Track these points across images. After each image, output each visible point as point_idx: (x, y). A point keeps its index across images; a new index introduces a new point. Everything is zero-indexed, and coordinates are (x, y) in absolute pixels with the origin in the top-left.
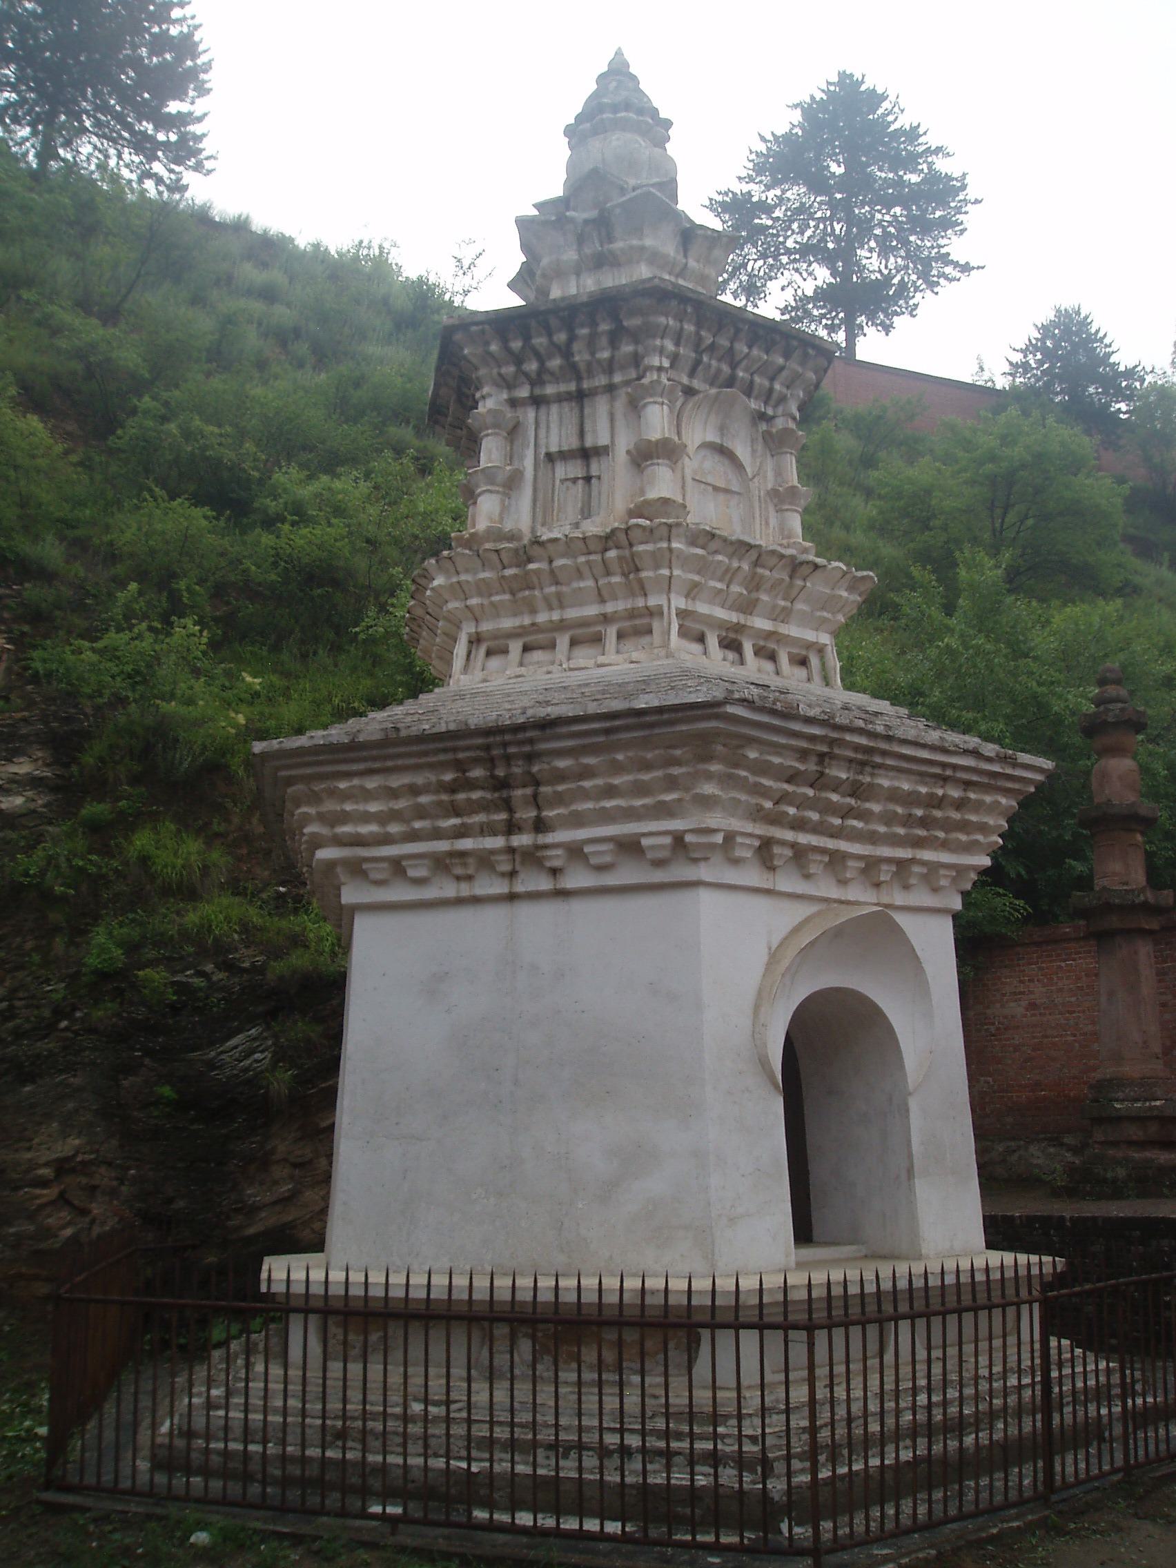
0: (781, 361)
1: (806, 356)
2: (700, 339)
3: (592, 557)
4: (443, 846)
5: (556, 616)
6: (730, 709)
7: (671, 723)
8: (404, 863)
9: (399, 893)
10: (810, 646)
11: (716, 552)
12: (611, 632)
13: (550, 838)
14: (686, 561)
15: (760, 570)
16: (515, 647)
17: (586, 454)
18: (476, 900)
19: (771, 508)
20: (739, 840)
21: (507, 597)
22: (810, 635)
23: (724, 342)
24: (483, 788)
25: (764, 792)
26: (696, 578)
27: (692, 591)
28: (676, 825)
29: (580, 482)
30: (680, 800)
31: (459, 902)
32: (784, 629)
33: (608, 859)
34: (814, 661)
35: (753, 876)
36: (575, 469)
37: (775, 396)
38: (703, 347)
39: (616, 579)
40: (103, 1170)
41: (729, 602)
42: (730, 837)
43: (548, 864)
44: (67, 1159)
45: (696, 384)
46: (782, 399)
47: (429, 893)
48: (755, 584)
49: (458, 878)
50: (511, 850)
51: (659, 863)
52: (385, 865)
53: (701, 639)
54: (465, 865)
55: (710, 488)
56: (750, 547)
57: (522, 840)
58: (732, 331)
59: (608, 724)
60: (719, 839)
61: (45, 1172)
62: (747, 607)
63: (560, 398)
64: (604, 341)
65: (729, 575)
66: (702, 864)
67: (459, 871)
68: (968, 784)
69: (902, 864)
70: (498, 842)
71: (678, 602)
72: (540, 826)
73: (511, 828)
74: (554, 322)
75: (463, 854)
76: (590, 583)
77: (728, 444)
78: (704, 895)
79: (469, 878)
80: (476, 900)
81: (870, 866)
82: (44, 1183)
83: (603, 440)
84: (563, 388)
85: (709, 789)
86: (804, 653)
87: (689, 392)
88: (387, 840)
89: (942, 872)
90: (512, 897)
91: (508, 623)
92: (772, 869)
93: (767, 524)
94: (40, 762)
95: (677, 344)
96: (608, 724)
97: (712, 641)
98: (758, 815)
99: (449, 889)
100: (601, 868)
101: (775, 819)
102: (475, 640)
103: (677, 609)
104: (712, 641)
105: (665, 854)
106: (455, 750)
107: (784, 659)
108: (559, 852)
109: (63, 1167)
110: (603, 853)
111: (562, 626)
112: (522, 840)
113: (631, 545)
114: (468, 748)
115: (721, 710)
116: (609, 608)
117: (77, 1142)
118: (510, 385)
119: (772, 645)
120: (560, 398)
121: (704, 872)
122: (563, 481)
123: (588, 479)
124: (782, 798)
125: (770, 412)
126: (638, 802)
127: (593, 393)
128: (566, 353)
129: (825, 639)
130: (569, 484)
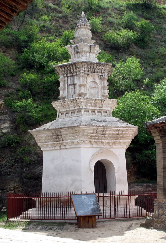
0: (102, 68)
1: (106, 66)
2: (88, 67)
3: (72, 102)
4: (52, 143)
5: (69, 109)
8: (48, 145)
10: (107, 110)
11: (88, 100)
13: (64, 142)
14: (84, 102)
15: (96, 102)
16: (65, 113)
17: (74, 85)
18: (57, 149)
19: (102, 89)
20: (86, 141)
22: (107, 109)
23: (92, 67)
24: (56, 136)
25: (89, 136)
26: (86, 104)
27: (86, 106)
28: (78, 140)
29: (74, 88)
31: (55, 150)
34: (108, 112)
35: (89, 145)
36: (71, 87)
37: (102, 72)
38: (89, 68)
39: (75, 105)
40: (20, 188)
42: (84, 141)
44: (15, 187)
45: (89, 73)
46: (104, 73)
47: (51, 149)
48: (95, 104)
51: (76, 145)
53: (89, 111)
54: (55, 145)
55: (92, 88)
58: (93, 65)
60: (83, 141)
61: (12, 189)
62: (95, 106)
63: (70, 76)
64: (75, 69)
65: (91, 103)
67: (54, 146)
71: (84, 107)
72: (63, 140)
73: (59, 141)
74: (67, 66)
75: (54, 144)
76: (72, 105)
77: (95, 81)
78: (82, 148)
79: (56, 147)
80: (57, 149)
81: (108, 143)
82: (12, 190)
83: (76, 83)
84: (70, 75)
87: (88, 74)
90: (61, 149)
91: (63, 110)
93: (101, 92)
95: (85, 68)
97: (90, 112)
98: (88, 138)
100: (70, 145)
101: (91, 139)
104: (90, 112)
105: (77, 144)
108: (65, 143)
109: (15, 188)
110: (70, 144)
111: (70, 110)
117: (16, 184)
118: (64, 75)
119: (100, 111)
120: (70, 76)
121: (81, 146)
122: (71, 88)
123: (75, 88)
125: (102, 74)
127: (75, 75)
128: (70, 71)
130: (72, 89)
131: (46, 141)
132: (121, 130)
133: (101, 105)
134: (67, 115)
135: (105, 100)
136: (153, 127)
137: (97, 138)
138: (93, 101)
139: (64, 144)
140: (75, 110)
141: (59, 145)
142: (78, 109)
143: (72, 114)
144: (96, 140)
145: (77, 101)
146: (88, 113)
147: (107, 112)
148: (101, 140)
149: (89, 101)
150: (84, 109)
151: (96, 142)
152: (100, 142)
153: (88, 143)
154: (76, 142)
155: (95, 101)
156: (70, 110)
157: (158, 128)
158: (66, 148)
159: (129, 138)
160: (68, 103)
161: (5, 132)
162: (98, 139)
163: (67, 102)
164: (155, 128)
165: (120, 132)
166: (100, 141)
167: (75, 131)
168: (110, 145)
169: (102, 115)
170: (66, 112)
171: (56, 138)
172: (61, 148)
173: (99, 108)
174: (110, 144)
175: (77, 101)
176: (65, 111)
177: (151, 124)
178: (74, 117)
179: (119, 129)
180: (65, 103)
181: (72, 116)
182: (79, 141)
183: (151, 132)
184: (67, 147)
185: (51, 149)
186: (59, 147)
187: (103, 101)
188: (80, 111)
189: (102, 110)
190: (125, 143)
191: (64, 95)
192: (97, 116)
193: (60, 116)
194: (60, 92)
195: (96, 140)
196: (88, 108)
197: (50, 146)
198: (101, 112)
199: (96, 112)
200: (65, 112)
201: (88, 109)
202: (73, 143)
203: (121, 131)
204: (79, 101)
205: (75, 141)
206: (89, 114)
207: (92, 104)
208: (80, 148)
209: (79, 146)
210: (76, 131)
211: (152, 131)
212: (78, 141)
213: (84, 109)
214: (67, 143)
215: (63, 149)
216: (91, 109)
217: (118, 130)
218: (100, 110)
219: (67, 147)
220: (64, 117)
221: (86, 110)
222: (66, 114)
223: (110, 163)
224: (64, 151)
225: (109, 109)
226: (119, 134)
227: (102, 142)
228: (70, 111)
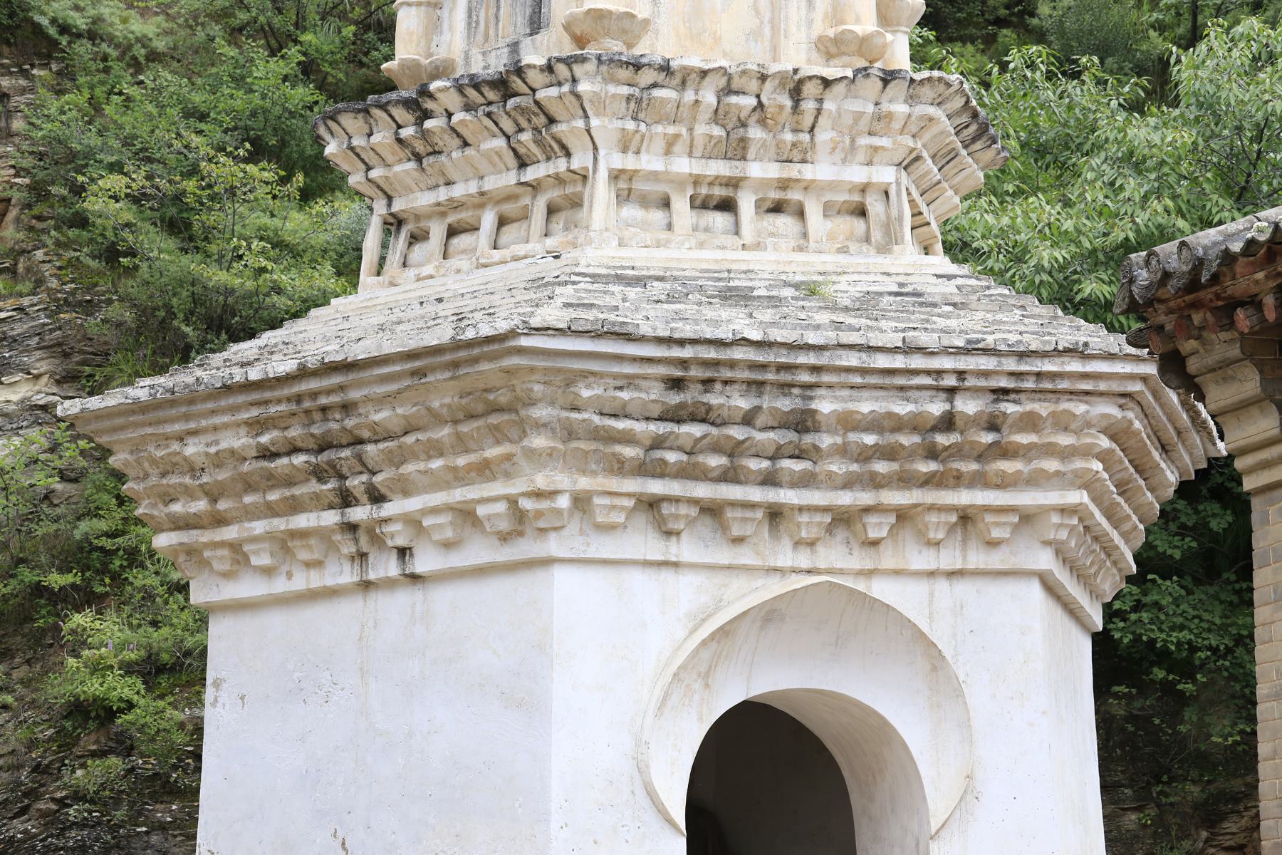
3: (493, 108)
4: (280, 524)
5: (473, 188)
6: (525, 342)
7: (475, 360)
8: (246, 548)
9: (247, 588)
10: (864, 189)
11: (655, 85)
12: (488, 220)
13: (388, 509)
16: (437, 231)
18: (331, 593)
20: (597, 501)
21: (412, 165)
22: (857, 174)
24: (307, 451)
25: (627, 438)
28: (514, 488)
30: (509, 457)
32: (808, 172)
33: (449, 534)
34: (875, 206)
35: (642, 542)
39: (526, 137)
41: (698, 151)
42: (581, 502)
43: (390, 543)
47: (280, 585)
49: (308, 565)
50: (352, 528)
51: (504, 538)
52: (225, 552)
53: (666, 204)
56: (704, 73)
57: (359, 514)
59: (417, 364)
60: (563, 502)
62: (738, 150)
66: (553, 535)
68: (1001, 394)
69: (903, 516)
70: (330, 518)
71: (611, 159)
72: (377, 498)
73: (346, 500)
75: (302, 534)
76: (500, 143)
78: (562, 577)
80: (331, 593)
81: (843, 519)
85: (539, 441)
86: (856, 198)
88: (220, 521)
89: (989, 518)
91: (424, 200)
92: (669, 534)
94: (45, 379)
96: (417, 364)
97: (681, 204)
98: (620, 467)
99: (301, 581)
100: (448, 545)
102: (394, 224)
103: (610, 171)
104: (681, 204)
105: (504, 525)
106: (266, 402)
107: (814, 211)
112: (359, 514)
113: (534, 91)
114: (279, 401)
115: (513, 343)
116: (531, 174)
119: (794, 195)
121: (553, 546)
124: (658, 443)
126: (461, 461)
129: (886, 174)
131: (222, 505)
132: (982, 383)
133: (796, 131)
134: (460, 241)
135: (827, 83)
136: (1196, 305)
137: (715, 461)
138: (709, 98)
139: (389, 529)
140: (535, 187)
141: (348, 548)
142: (559, 180)
143: (509, 232)
144: (702, 491)
145: (540, 95)
146: (658, 216)
147: (862, 212)
148: (769, 480)
149: (657, 93)
150: (616, 176)
151: (712, 510)
152: (752, 506)
153: (620, 518)
154: (501, 507)
155: (728, 90)
156: (482, 194)
157: (1240, 314)
158: (415, 578)
159: (1079, 464)
160: (455, 119)
161: (326, 527)
162: (730, 476)
163: (450, 115)
164: (1214, 310)
165: (968, 406)
166: (756, 494)
167: (485, 390)
168: (875, 543)
169: (805, 235)
170: (452, 219)
171: (319, 474)
172: (372, 576)
173: (772, 171)
174: (873, 534)
175: (540, 95)
176: (440, 210)
177: (1167, 275)
178: (516, 259)
179: (961, 374)
180: (428, 124)
181: (497, 255)
182: (524, 494)
183: (1193, 365)
184: (423, 562)
185: (280, 585)
186: (347, 566)
187: (811, 89)
188: (576, 203)
189: (808, 187)
190: (1027, 518)
191: (441, 54)
192: (758, 246)
193: (394, 258)
194: (401, 15)
195: (702, 491)
196: (650, 162)
197: (262, 559)
198: (801, 214)
199: (746, 204)
200: (443, 215)
201: (654, 176)
202: (466, 515)
203: (976, 390)
204: (554, 92)
205: (489, 496)
206: (669, 227)
207: (701, 129)
208: (540, 575)
209: (526, 548)
210: (491, 397)
211: (1195, 352)
212: (512, 501)
213: (616, 176)
214: (413, 522)
215: (389, 584)
216: (697, 181)
217: (951, 381)
218: (784, 184)
219: (423, 562)
220: (428, 270)
221: (638, 185)
222: (452, 232)
223: (882, 731)
224: (397, 606)
225: (886, 174)
226: (959, 422)
227: (775, 514)
228: (481, 206)
